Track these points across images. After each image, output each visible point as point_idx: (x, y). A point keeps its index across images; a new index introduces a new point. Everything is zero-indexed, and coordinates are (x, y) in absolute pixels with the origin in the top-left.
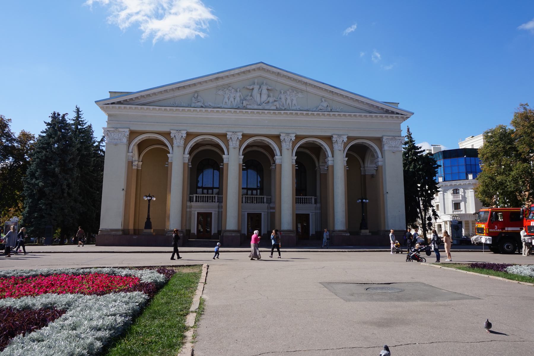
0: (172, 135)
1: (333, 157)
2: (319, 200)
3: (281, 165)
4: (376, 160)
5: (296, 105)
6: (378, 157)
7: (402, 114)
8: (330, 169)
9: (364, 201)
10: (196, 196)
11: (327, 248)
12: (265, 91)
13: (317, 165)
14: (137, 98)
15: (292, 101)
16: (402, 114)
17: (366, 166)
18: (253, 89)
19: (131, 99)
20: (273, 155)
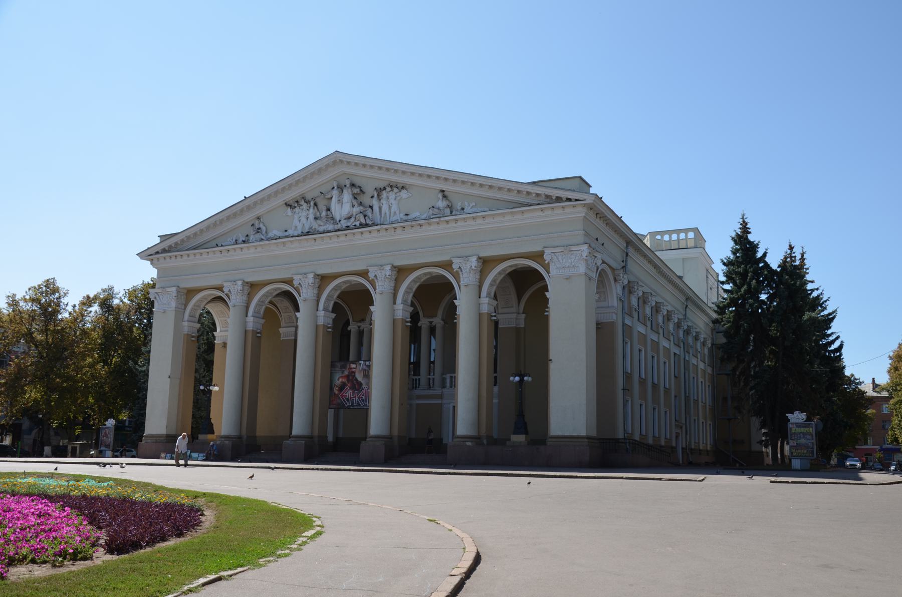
5: (397, 212)
7: (576, 200)
11: (267, 462)
14: (182, 241)
15: (390, 207)
16: (576, 200)
19: (176, 244)
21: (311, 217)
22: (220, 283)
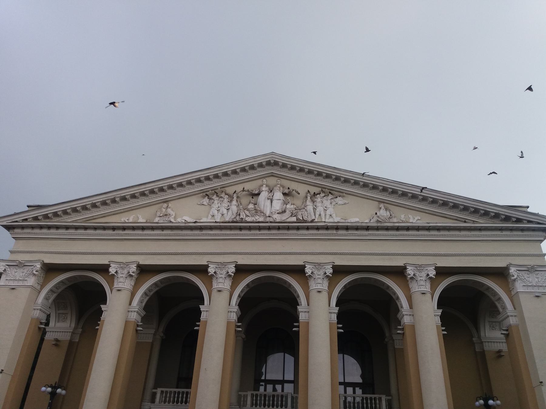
0: (112, 270)
1: (411, 307)
2: (395, 405)
3: (308, 323)
4: (500, 317)
5: (334, 215)
6: (504, 308)
8: (408, 332)
9: (491, 402)
10: (162, 392)
12: (278, 195)
13: (387, 334)
17: (482, 334)
18: (258, 194)
20: (294, 302)
21: (234, 208)
22: (106, 262)
